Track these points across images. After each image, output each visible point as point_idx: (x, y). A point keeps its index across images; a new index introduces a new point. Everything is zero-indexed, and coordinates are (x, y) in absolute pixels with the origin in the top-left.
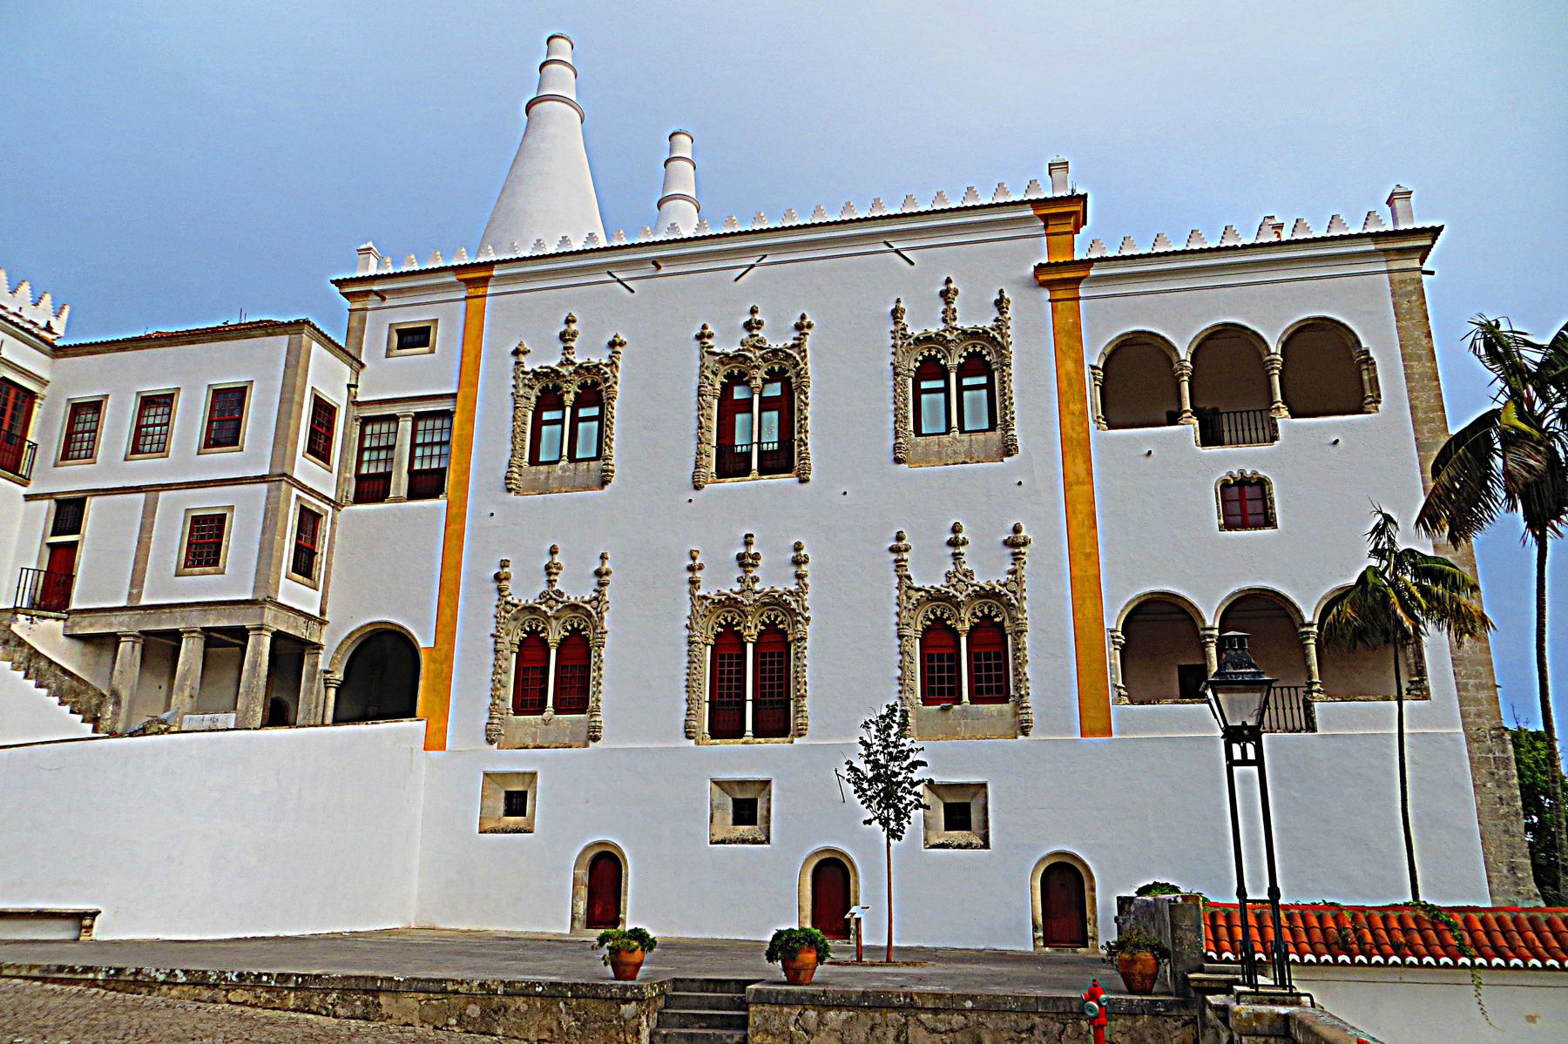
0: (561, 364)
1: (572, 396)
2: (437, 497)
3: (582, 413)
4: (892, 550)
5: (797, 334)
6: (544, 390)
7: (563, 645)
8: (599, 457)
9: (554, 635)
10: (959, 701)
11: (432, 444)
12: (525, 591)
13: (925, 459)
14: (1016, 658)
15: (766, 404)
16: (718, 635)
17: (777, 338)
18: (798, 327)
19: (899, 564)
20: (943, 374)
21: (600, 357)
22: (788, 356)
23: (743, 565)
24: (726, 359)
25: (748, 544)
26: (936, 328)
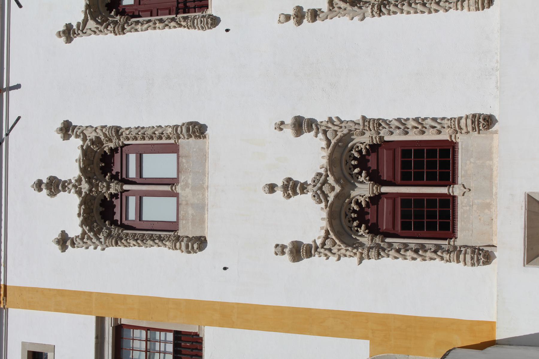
0: (79, 193)
2: (201, 339)
7: (375, 178)
9: (363, 190)
12: (310, 219)
21: (74, 147)
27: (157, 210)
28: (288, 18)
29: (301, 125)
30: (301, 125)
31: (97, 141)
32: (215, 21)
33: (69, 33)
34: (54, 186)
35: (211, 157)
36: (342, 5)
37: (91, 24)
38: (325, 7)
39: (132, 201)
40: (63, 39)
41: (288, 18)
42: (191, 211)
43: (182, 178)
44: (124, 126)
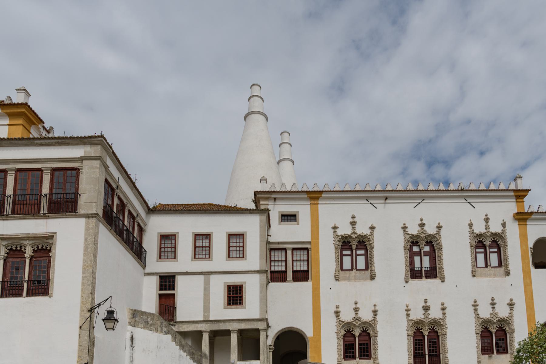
0: (352, 234)
1: (355, 246)
3: (359, 252)
4: (473, 306)
5: (437, 230)
6: (344, 242)
8: (367, 268)
10: (493, 353)
11: (300, 260)
13: (481, 275)
14: (510, 340)
15: (426, 253)
16: (415, 333)
17: (430, 230)
18: (438, 227)
19: (476, 310)
20: (484, 247)
21: (367, 232)
22: (434, 237)
23: (424, 310)
24: (413, 236)
25: (426, 302)
26: (483, 231)
27: (347, 261)
28: (407, 307)
29: (375, 312)
30: (375, 312)
31: (369, 240)
32: (407, 282)
33: (405, 228)
34: (353, 224)
35: (365, 282)
36: (411, 324)
37: (408, 237)
38: (410, 318)
39: (349, 252)
40: (403, 226)
41: (407, 307)
42: (348, 275)
43: (358, 272)
44: (374, 250)
